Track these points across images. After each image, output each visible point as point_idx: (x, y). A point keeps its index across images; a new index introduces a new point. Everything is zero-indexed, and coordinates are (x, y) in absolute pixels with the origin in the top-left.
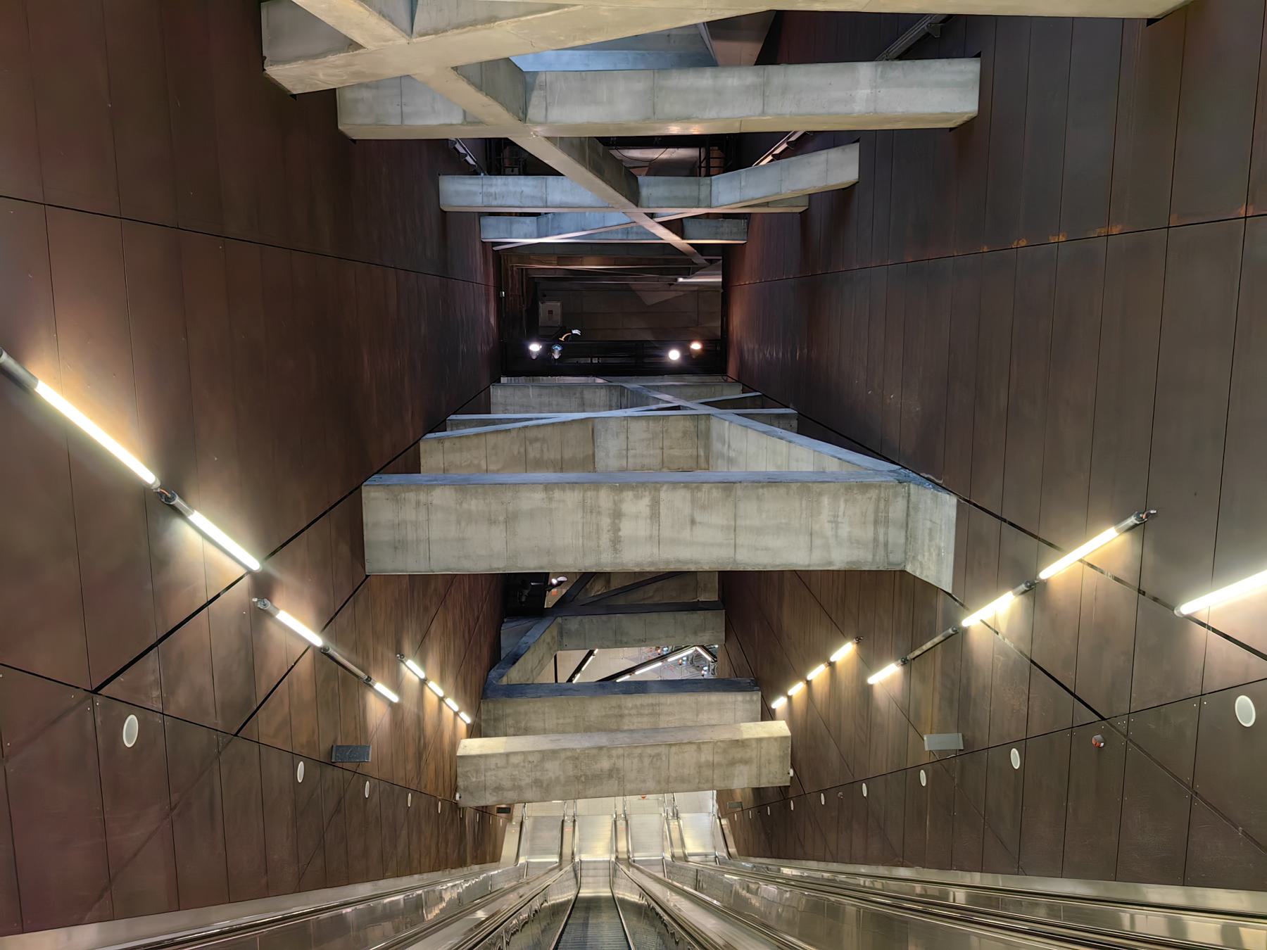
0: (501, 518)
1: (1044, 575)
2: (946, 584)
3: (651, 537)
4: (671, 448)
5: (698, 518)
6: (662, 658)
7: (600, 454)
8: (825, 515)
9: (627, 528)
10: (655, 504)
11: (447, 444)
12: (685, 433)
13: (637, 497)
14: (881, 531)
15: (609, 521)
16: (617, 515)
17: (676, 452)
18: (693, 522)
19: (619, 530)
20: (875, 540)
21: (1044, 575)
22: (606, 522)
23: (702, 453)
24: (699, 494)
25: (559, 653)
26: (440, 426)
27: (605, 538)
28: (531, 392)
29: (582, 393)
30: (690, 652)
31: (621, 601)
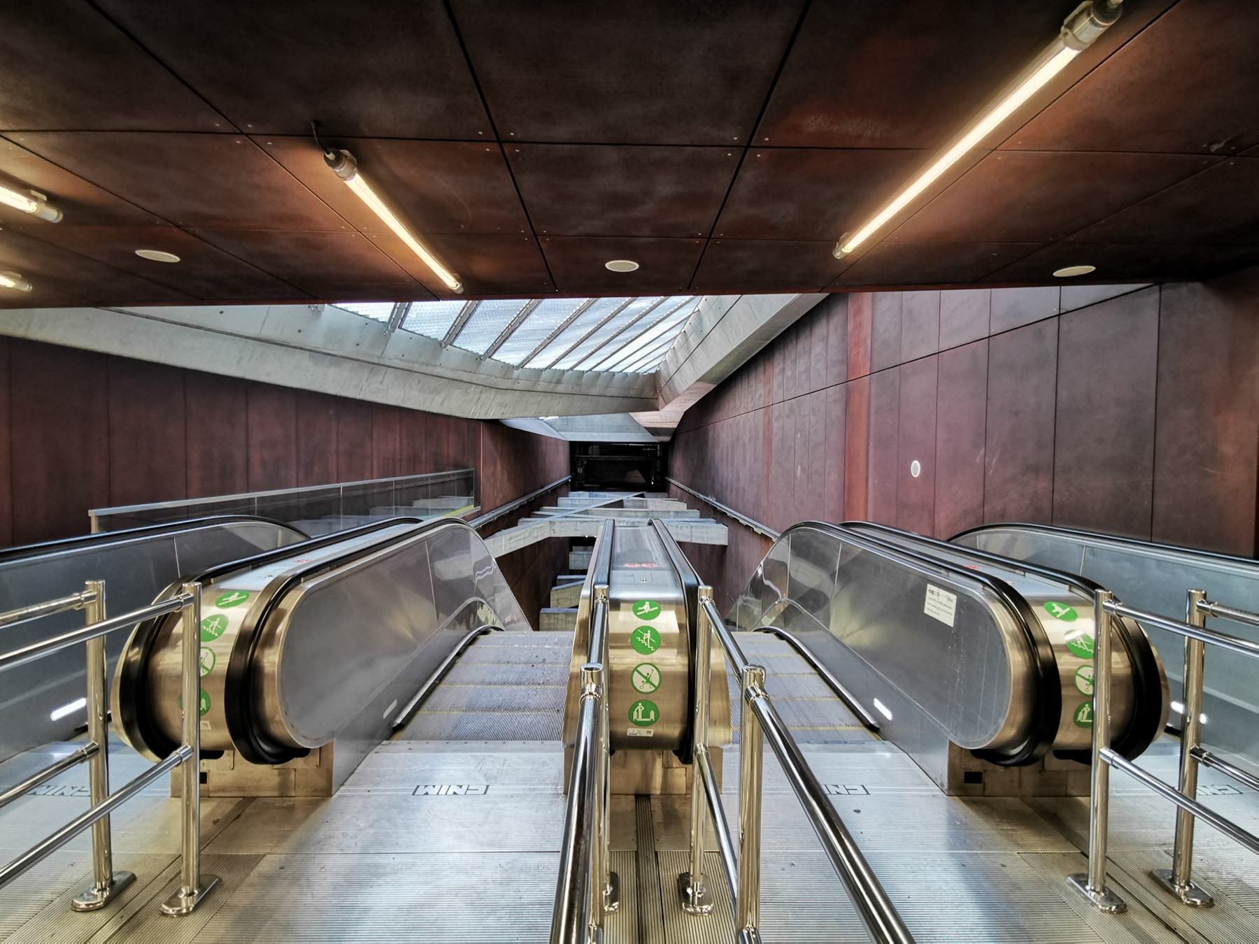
26: (555, 585)
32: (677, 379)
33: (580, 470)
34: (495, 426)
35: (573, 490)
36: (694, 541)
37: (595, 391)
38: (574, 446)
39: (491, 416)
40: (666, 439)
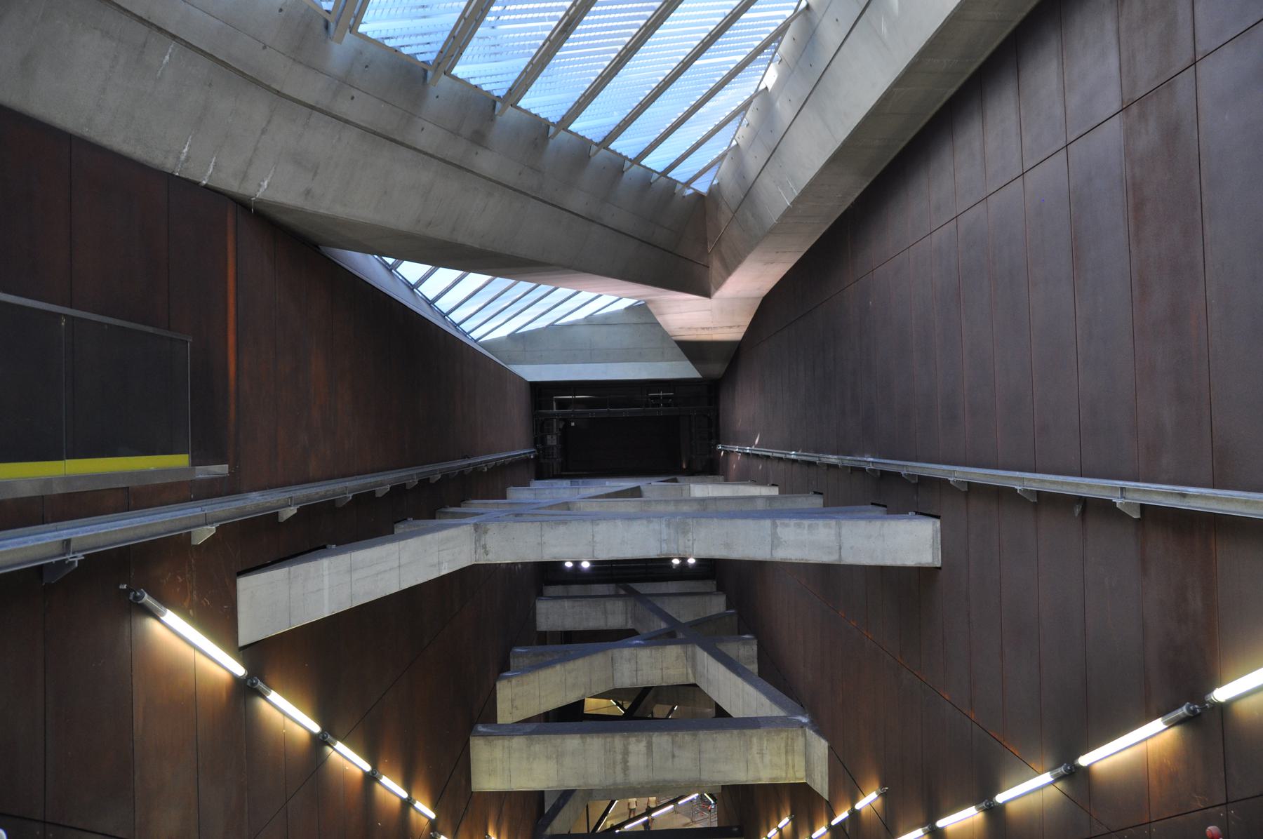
1: (858, 806)
2: (826, 797)
5: (676, 753)
6: (674, 801)
8: (755, 749)
9: (632, 760)
10: (649, 746)
11: (514, 681)
12: (677, 658)
13: (638, 741)
14: (790, 758)
16: (626, 753)
18: (673, 756)
20: (787, 764)
21: (858, 806)
22: (619, 757)
25: (590, 804)
27: (619, 768)
28: (567, 604)
30: (695, 796)
32: (767, 182)
33: (552, 440)
34: (301, 249)
35: (540, 476)
36: (850, 559)
37: (577, 202)
38: (541, 392)
39: (269, 185)
40: (717, 369)
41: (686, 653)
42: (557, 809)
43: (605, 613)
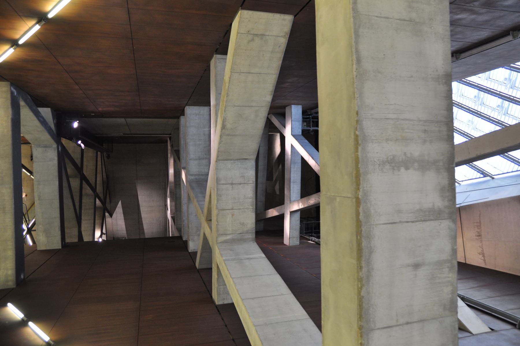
0: (414, 15)
3: (399, 211)
4: (233, 215)
7: (229, 164)
9: (409, 178)
15: (416, 154)
17: (229, 219)
18: (416, 266)
19: (407, 168)
23: (229, 237)
24: (446, 270)
29: (206, 158)
31: (65, 184)
41: (247, 232)
42: (37, 115)
43: (200, 159)
